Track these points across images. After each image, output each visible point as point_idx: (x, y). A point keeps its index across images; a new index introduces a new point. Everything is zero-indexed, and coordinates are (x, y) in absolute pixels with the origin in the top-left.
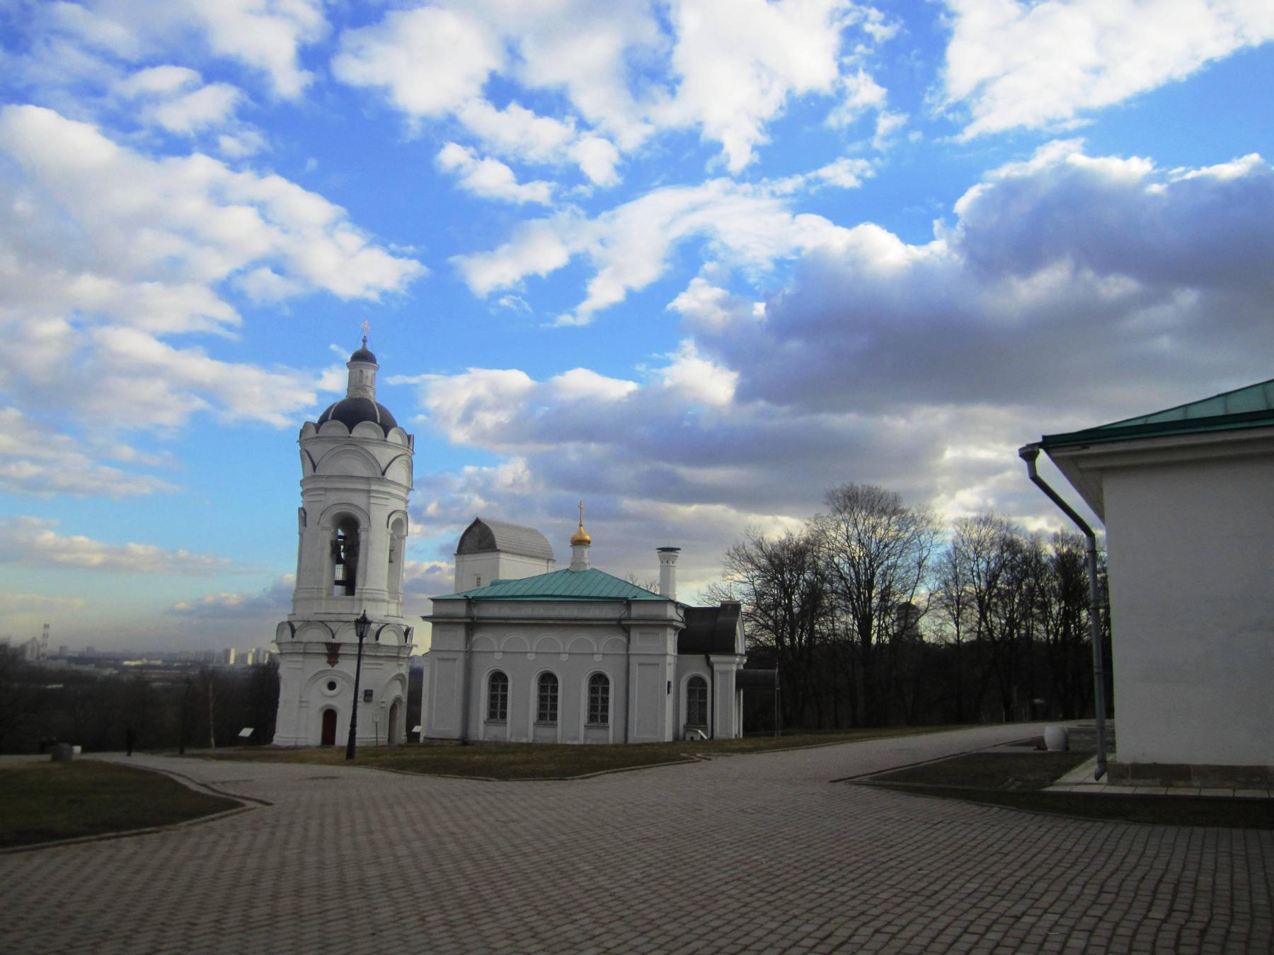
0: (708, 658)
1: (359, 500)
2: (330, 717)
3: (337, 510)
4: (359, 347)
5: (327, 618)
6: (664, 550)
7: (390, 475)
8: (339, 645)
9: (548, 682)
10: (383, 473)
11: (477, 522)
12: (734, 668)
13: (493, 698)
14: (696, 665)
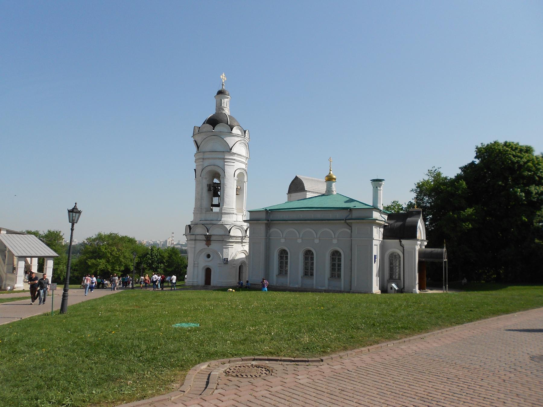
0: (401, 242)
1: (219, 162)
2: (208, 272)
3: (209, 168)
4: (220, 89)
6: (374, 180)
8: (211, 235)
9: (308, 254)
11: (296, 177)
12: (418, 248)
14: (394, 244)
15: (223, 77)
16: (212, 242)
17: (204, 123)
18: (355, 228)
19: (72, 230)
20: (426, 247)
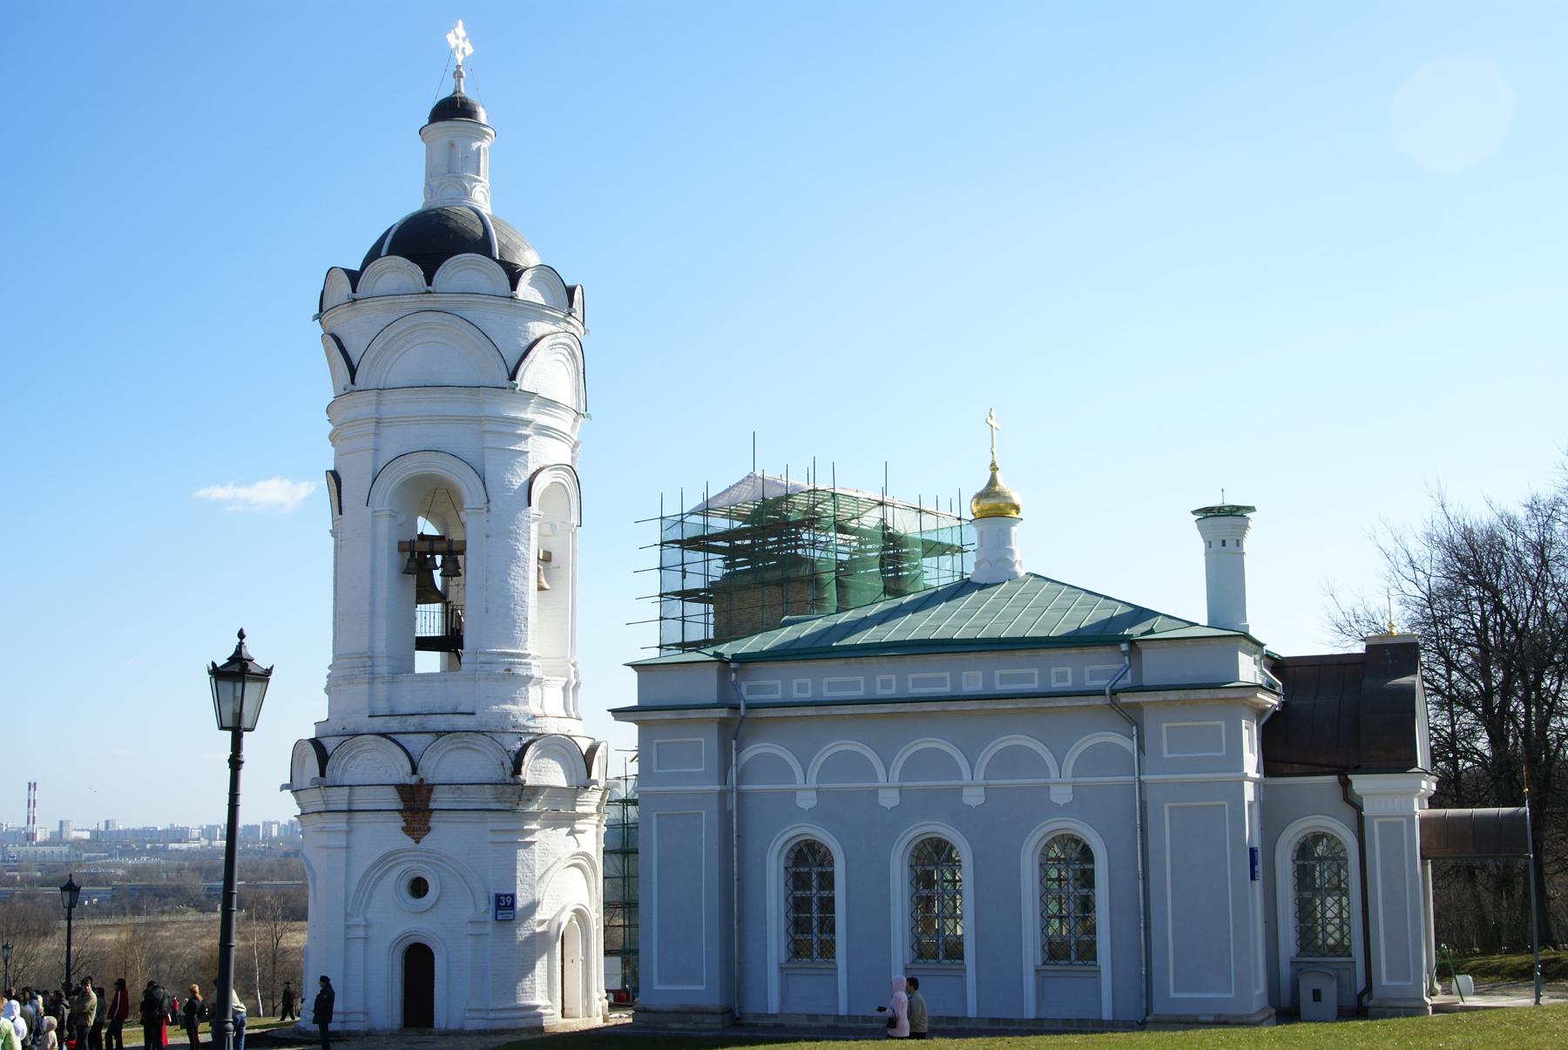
0: (1346, 784)
4: (446, 93)
5: (394, 725)
6: (1207, 513)
7: (528, 379)
10: (513, 377)
13: (798, 906)
15: (459, 40)
16: (435, 821)
17: (374, 254)
18: (1162, 728)
19: (235, 763)
20: (1434, 802)
